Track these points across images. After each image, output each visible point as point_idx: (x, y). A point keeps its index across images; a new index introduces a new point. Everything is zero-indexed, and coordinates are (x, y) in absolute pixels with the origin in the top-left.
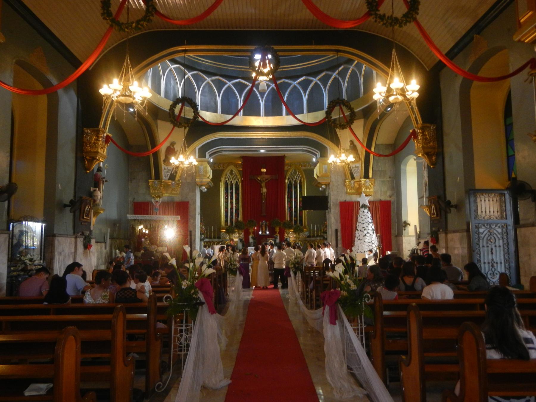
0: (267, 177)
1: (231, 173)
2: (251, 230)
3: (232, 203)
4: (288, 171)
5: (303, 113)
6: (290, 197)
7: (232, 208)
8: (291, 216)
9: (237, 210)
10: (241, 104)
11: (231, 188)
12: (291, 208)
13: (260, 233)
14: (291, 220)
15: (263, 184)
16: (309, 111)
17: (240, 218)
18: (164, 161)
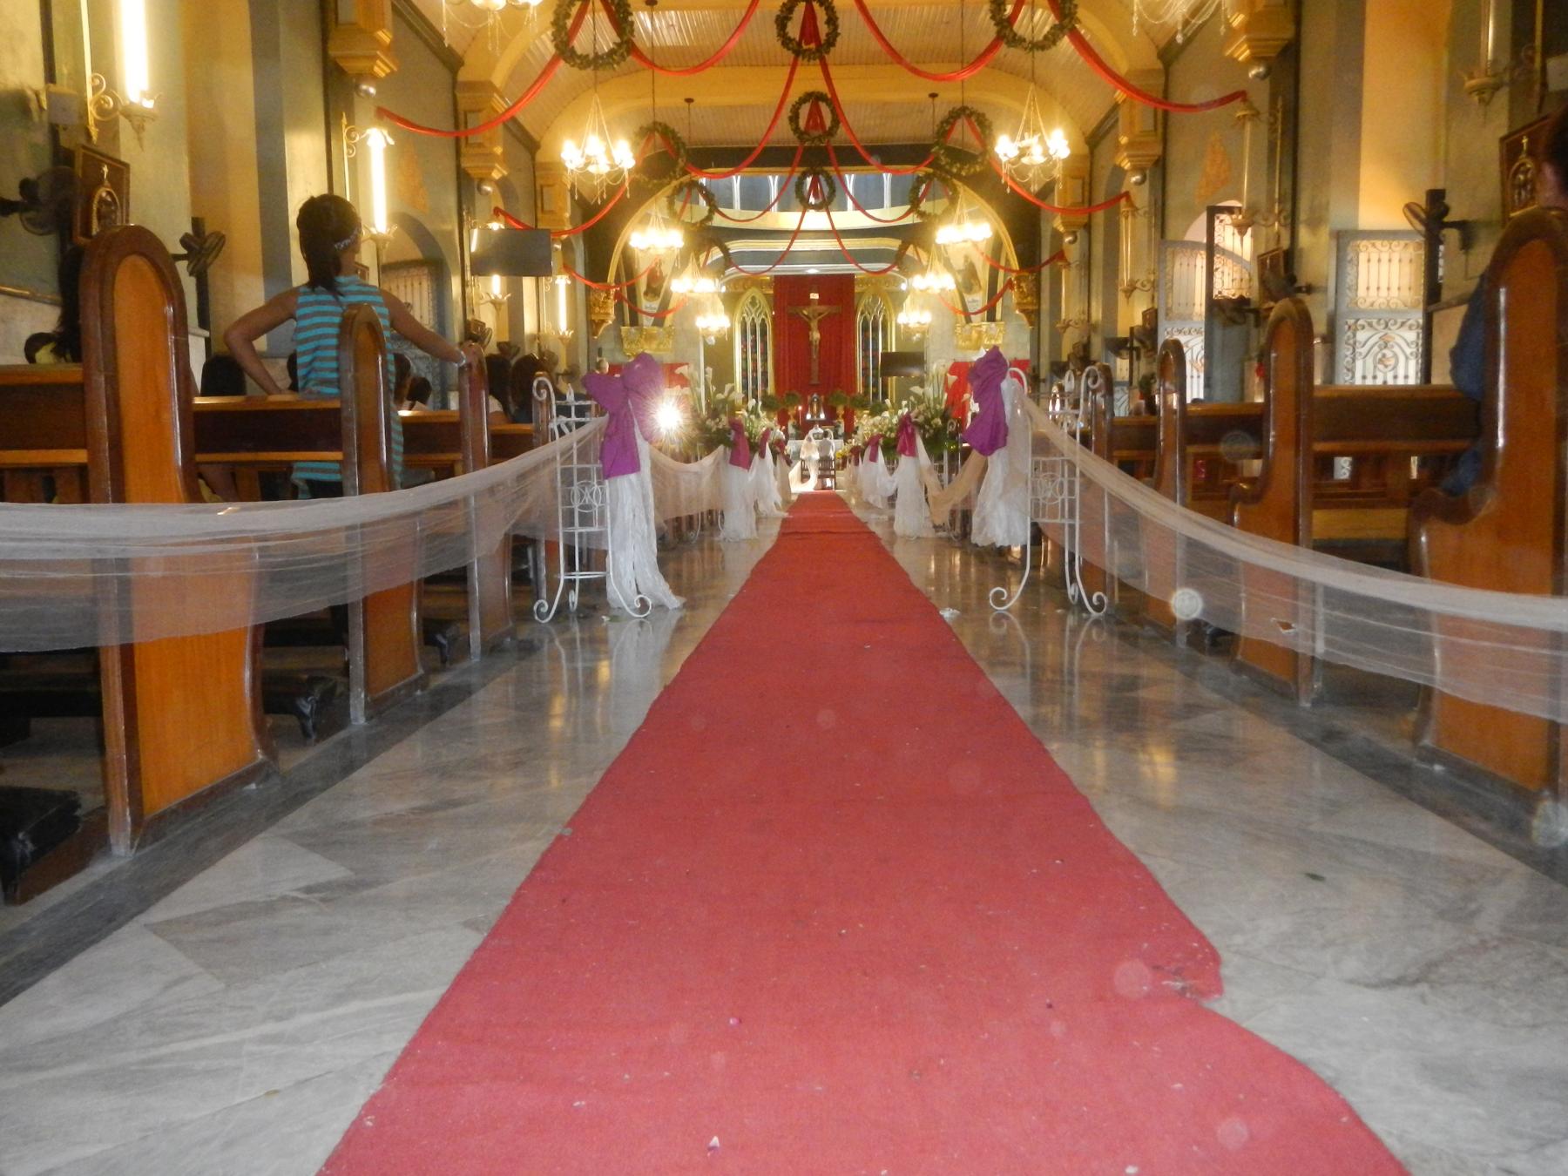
0: (822, 308)
1: (753, 303)
2: (791, 412)
3: (754, 361)
4: (862, 294)
6: (865, 349)
7: (755, 370)
8: (866, 386)
9: (765, 373)
10: (774, 193)
11: (754, 332)
12: (865, 369)
13: (809, 417)
14: (866, 393)
15: (814, 324)
16: (893, 204)
17: (771, 389)
18: (646, 294)
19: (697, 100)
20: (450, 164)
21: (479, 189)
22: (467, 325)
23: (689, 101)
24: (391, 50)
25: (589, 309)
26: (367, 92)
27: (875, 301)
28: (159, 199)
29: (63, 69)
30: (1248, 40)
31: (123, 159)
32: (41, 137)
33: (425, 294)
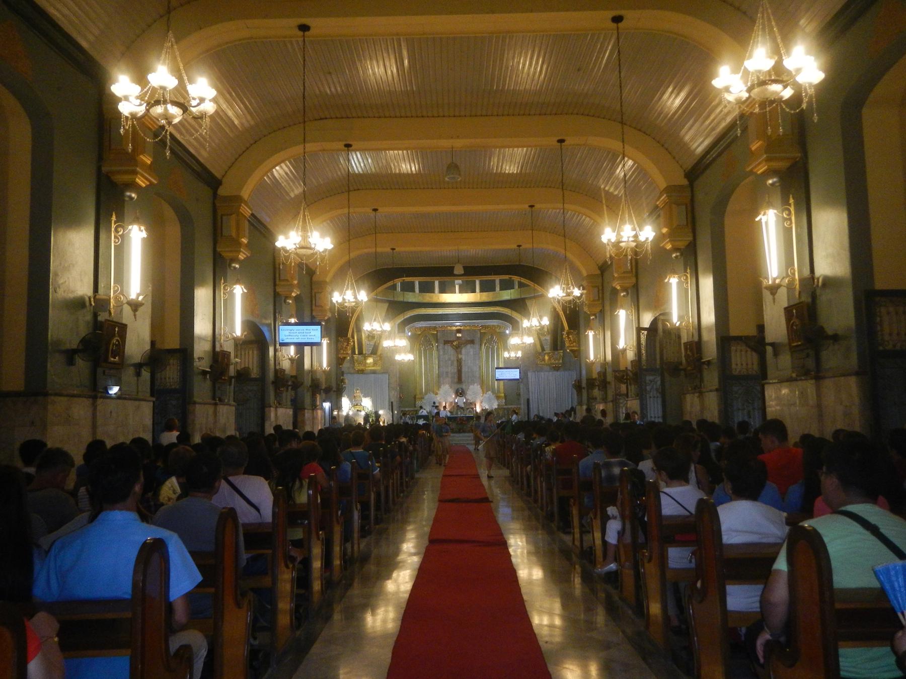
5: (493, 289)
16: (501, 289)
19: (397, 249)
20: (270, 290)
21: (285, 302)
22: (276, 371)
23: (393, 249)
24: (247, 246)
25: (337, 351)
26: (235, 268)
27: (492, 338)
28: (138, 338)
29: (101, 285)
30: (670, 241)
31: (124, 322)
32: (89, 317)
33: (255, 356)
